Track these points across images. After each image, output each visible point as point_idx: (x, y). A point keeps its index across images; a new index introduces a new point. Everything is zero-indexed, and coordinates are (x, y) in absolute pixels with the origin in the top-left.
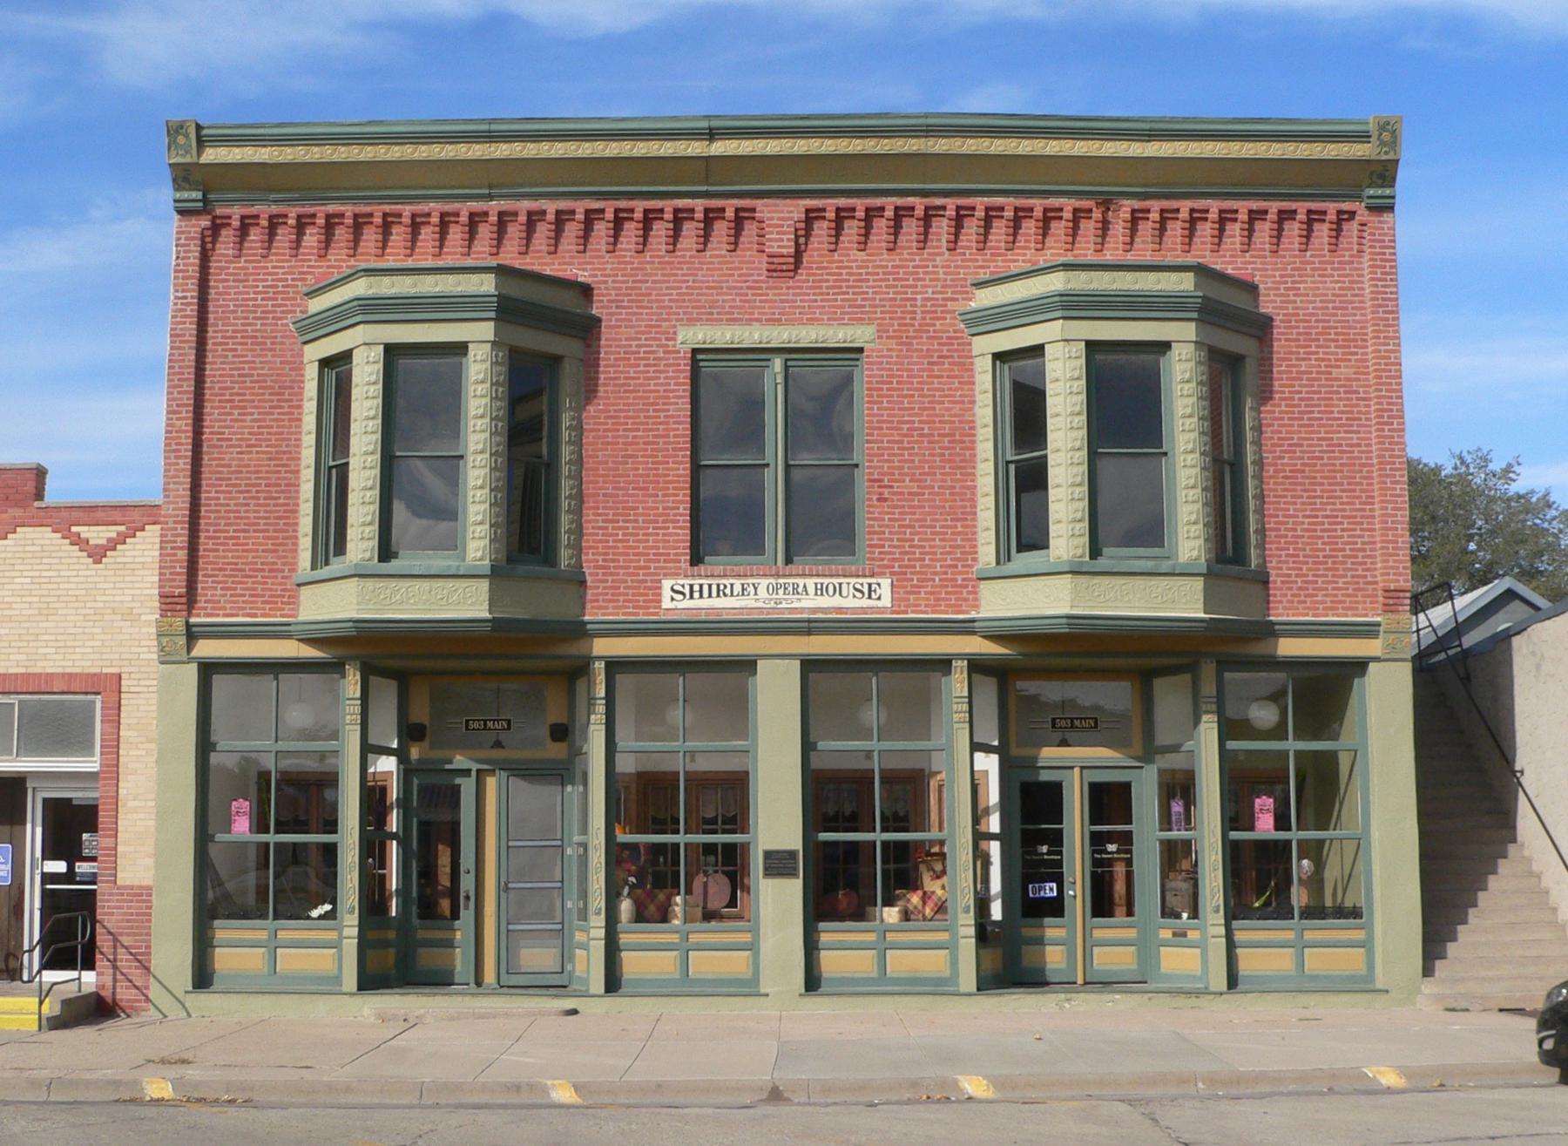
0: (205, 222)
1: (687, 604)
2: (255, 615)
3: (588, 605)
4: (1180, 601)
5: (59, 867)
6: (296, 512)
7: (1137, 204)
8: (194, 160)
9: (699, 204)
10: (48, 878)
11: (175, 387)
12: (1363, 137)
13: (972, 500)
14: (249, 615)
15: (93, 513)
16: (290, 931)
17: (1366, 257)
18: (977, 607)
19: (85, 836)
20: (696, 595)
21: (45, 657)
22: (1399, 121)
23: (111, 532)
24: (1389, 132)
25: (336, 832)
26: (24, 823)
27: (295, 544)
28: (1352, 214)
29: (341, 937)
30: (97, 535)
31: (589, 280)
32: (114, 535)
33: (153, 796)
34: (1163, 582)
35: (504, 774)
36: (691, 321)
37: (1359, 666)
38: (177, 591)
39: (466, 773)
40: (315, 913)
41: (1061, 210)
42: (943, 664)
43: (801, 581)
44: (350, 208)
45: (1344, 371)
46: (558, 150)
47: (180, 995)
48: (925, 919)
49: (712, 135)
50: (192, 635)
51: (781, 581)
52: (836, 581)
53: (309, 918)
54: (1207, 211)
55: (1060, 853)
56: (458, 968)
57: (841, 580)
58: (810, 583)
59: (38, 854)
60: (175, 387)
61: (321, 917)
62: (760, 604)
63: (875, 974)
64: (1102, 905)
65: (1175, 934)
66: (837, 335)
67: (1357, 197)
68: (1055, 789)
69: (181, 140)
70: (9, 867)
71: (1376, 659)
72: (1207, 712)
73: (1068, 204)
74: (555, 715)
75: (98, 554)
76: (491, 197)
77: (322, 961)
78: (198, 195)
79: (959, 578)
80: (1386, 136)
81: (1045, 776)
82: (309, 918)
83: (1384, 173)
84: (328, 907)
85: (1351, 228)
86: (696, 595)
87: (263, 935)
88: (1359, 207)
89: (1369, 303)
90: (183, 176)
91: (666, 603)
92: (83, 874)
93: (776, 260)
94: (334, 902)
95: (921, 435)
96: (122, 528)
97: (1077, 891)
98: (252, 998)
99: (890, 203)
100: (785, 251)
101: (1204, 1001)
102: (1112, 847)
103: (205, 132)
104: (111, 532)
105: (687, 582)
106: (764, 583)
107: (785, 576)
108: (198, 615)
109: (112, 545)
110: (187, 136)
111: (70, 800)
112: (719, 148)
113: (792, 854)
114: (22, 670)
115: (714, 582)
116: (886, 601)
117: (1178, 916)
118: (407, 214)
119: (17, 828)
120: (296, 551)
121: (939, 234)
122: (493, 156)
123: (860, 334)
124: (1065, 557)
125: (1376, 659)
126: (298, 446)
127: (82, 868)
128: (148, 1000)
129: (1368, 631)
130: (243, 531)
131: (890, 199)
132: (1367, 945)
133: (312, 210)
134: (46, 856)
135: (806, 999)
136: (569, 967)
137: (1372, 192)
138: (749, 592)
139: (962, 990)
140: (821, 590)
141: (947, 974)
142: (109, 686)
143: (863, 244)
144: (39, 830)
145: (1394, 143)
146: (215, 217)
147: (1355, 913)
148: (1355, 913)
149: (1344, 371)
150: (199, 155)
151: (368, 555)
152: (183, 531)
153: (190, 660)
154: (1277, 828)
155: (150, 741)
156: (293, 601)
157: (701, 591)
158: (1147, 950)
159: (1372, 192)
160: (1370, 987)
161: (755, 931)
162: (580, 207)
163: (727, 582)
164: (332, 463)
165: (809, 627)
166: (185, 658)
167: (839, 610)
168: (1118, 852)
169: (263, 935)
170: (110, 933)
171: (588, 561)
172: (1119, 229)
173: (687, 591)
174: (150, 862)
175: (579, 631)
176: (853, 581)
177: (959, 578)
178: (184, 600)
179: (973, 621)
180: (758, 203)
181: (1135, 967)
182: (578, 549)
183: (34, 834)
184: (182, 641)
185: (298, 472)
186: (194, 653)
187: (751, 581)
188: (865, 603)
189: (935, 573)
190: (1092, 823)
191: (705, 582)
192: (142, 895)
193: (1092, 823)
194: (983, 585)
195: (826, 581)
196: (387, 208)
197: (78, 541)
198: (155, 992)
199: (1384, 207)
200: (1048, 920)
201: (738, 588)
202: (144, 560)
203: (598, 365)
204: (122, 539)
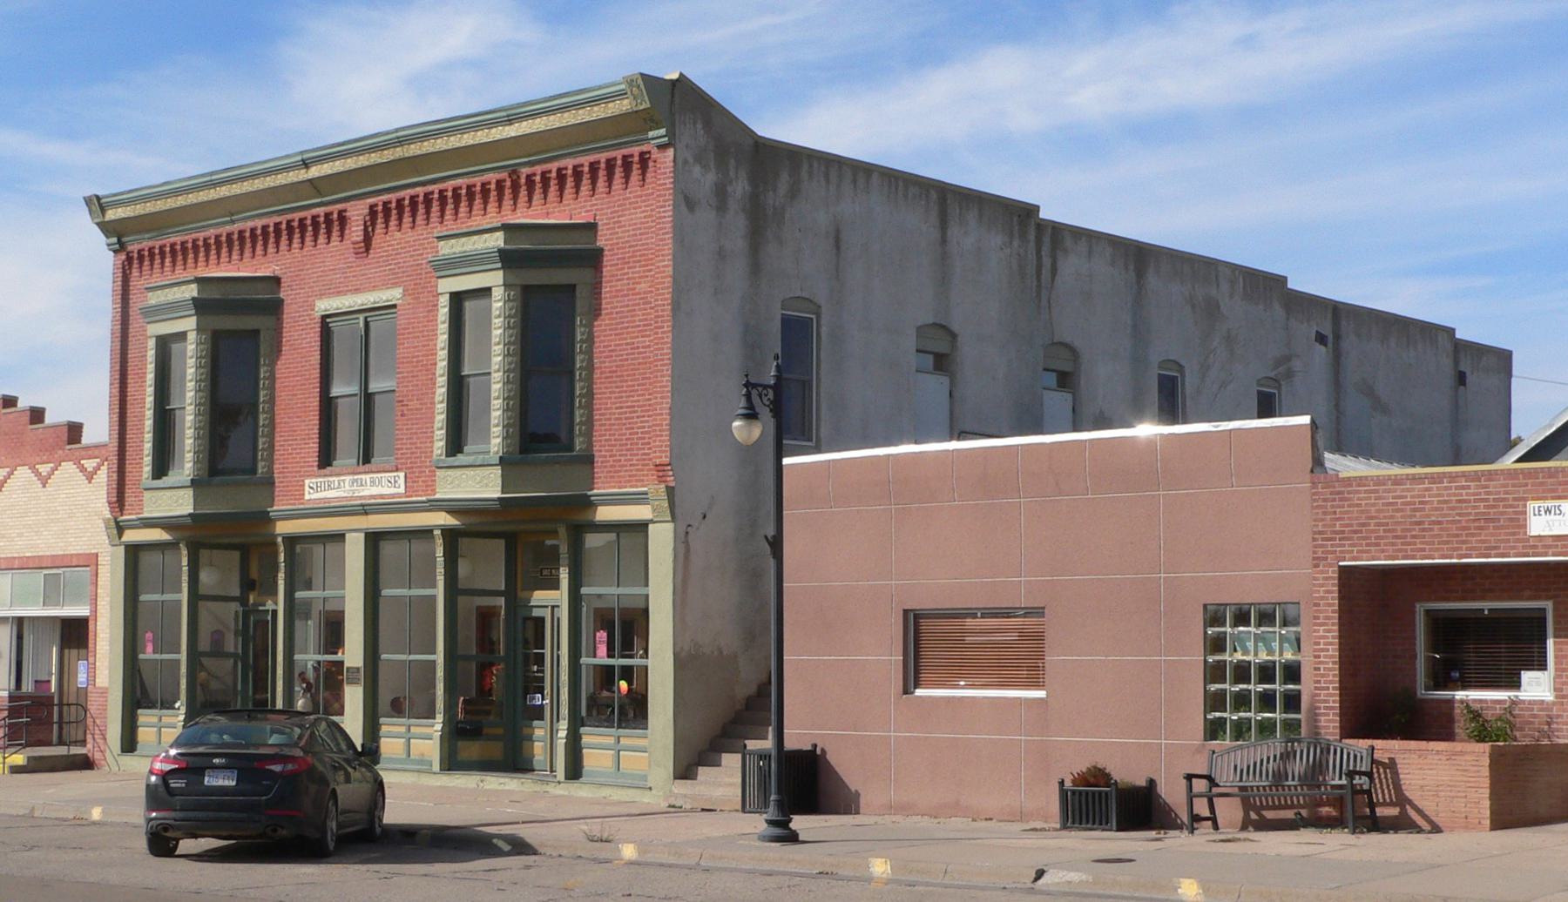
12: (620, 95)
36: (321, 296)
42: (425, 533)
45: (643, 286)
49: (306, 164)
50: (120, 529)
76: (233, 222)
81: (536, 613)
90: (107, 228)
91: (307, 497)
106: (348, 478)
112: (315, 172)
113: (358, 669)
116: (402, 490)
123: (393, 295)
125: (652, 521)
129: (640, 499)
149: (643, 286)
165: (365, 510)
175: (265, 519)
192: (104, 692)
198: (108, 754)
200: (536, 723)
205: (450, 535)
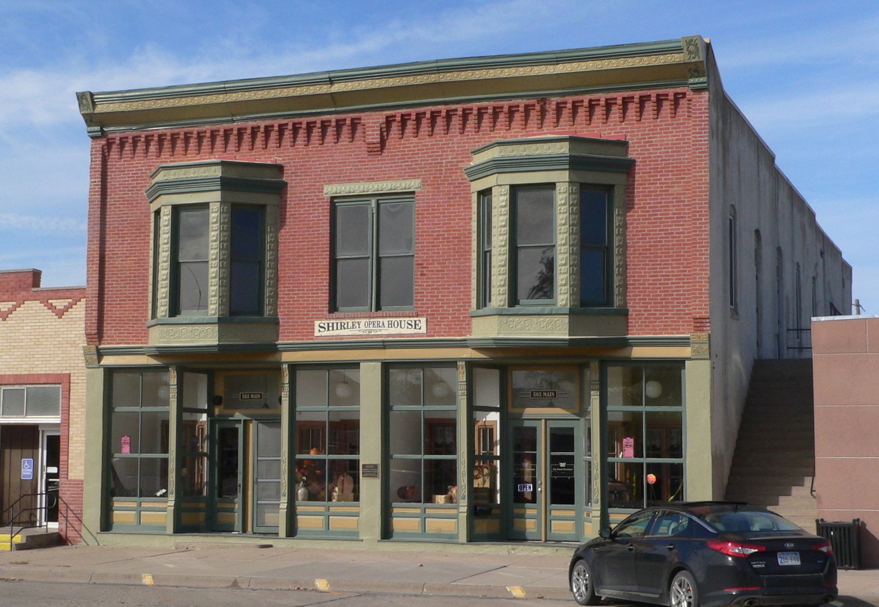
0: (104, 142)
1: (326, 333)
2: (129, 343)
3: (280, 335)
4: (553, 328)
8: (92, 111)
12: (678, 50)
15: (58, 293)
18: (470, 332)
23: (65, 303)
26: (38, 448)
28: (684, 94)
30: (60, 304)
34: (548, 319)
36: (331, 182)
38: (93, 332)
40: (158, 494)
41: (518, 106)
42: (451, 364)
43: (381, 320)
45: (676, 189)
47: (95, 535)
49: (331, 81)
50: (100, 355)
51: (372, 320)
52: (398, 319)
55: (572, 467)
58: (386, 321)
59: (45, 464)
61: (161, 496)
62: (361, 333)
63: (420, 531)
66: (400, 185)
67: (685, 84)
68: (534, 430)
71: (690, 359)
75: (60, 314)
76: (233, 121)
78: (97, 128)
80: (692, 48)
81: (527, 424)
84: (164, 491)
90: (90, 119)
91: (317, 334)
94: (167, 489)
95: (444, 238)
96: (70, 300)
97: (543, 489)
99: (428, 110)
100: (375, 141)
102: (563, 465)
104: (65, 303)
105: (326, 322)
106: (363, 321)
107: (373, 317)
110: (87, 99)
112: (337, 88)
113: (376, 466)
114: (27, 373)
115: (339, 321)
116: (424, 330)
118: (195, 132)
123: (413, 184)
125: (690, 359)
128: (81, 537)
129: (684, 342)
140: (391, 325)
143: (417, 132)
146: (108, 139)
149: (676, 189)
152: (95, 301)
153: (100, 367)
154: (635, 456)
156: (146, 335)
165: (384, 345)
167: (400, 335)
168: (566, 467)
169: (134, 505)
173: (326, 326)
174: (83, 467)
175: (274, 349)
180: (362, 115)
181: (574, 532)
182: (275, 305)
183: (42, 453)
184: (96, 357)
187: (357, 320)
188: (413, 331)
189: (449, 314)
192: (79, 484)
194: (474, 320)
195: (394, 320)
196: (186, 130)
197: (51, 307)
198: (84, 533)
201: (350, 325)
205: (471, 365)
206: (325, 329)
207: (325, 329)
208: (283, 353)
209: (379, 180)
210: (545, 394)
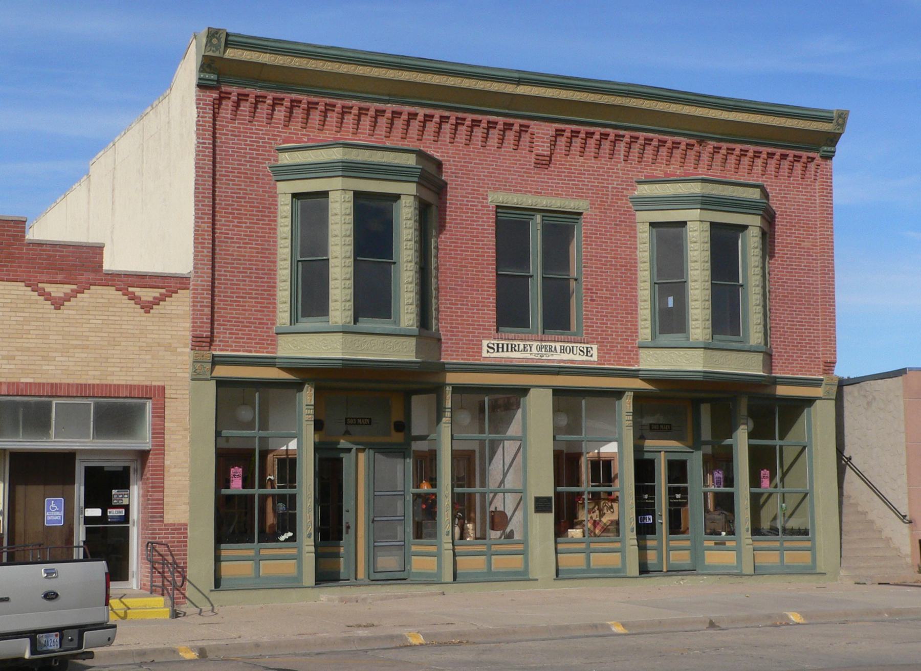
0: (215, 95)
1: (496, 355)
2: (251, 351)
3: (443, 353)
5: (96, 512)
6: (275, 287)
7: (716, 144)
8: (221, 55)
9: (501, 120)
10: (88, 520)
11: (199, 201)
12: (829, 120)
13: (635, 303)
14: (247, 351)
15: (143, 280)
16: (268, 549)
17: (817, 183)
18: (637, 363)
19: (114, 492)
20: (500, 350)
21: (113, 374)
22: (847, 112)
23: (156, 293)
24: (843, 117)
25: (295, 487)
26: (74, 484)
27: (275, 308)
28: (813, 159)
29: (439, 549)
30: (147, 294)
31: (441, 159)
32: (157, 295)
33: (187, 465)
34: (745, 355)
35: (372, 452)
36: (496, 189)
37: (809, 402)
38: (205, 334)
39: (349, 450)
40: (282, 538)
42: (618, 394)
43: (553, 344)
44: (339, 102)
45: (806, 244)
46: (466, 83)
47: (206, 592)
48: (595, 535)
49: (519, 82)
51: (544, 344)
52: (571, 345)
53: (278, 541)
54: (747, 151)
56: (342, 570)
57: (575, 345)
58: (558, 345)
59: (82, 504)
60: (199, 201)
61: (286, 540)
62: (533, 357)
63: (585, 568)
64: (676, 527)
65: (716, 544)
66: (571, 204)
67: (817, 151)
68: (652, 462)
69: (215, 41)
70: (62, 513)
71: (820, 398)
72: (743, 424)
73: (684, 141)
74: (397, 415)
75: (147, 307)
76: (388, 102)
77: (288, 568)
78: (213, 77)
79: (630, 346)
80: (840, 121)
81: (647, 456)
82: (278, 541)
83: (833, 139)
84: (290, 534)
85: (812, 166)
86: (500, 350)
87: (251, 553)
88: (817, 155)
89: (818, 209)
91: (485, 354)
92: (112, 517)
93: (540, 158)
94: (294, 530)
95: (611, 265)
96: (163, 291)
97: (663, 520)
98: (270, 591)
99: (598, 130)
100: (546, 153)
101: (744, 579)
102: (678, 496)
103: (230, 38)
104: (156, 293)
105: (496, 342)
107: (545, 341)
108: (215, 350)
109: (157, 301)
110: (219, 39)
111: (103, 467)
113: (549, 499)
114: (97, 382)
115: (510, 342)
116: (595, 358)
117: (720, 534)
118: (339, 105)
119: (67, 487)
120: (275, 312)
121: (619, 151)
122: (400, 78)
124: (701, 339)
125: (820, 398)
126: (275, 246)
127: (113, 513)
128: (185, 597)
129: (816, 383)
130: (242, 297)
131: (597, 129)
132: (812, 549)
133: (282, 96)
134: (89, 504)
135: (317, 591)
136: (408, 568)
137: (825, 148)
138: (528, 349)
139: (446, 581)
140: (563, 350)
141: (620, 566)
142: (157, 394)
144: (82, 488)
145: (842, 125)
146: (221, 92)
147: (805, 532)
148: (805, 532)
149: (806, 244)
150: (224, 52)
151: (411, 322)
152: (207, 295)
153: (212, 378)
155: (185, 430)
156: (274, 343)
157: (503, 348)
158: (697, 553)
159: (825, 148)
160: (813, 571)
161: (812, 540)
162: (438, 113)
163: (516, 343)
164: (299, 259)
166: (209, 377)
167: (572, 361)
168: (681, 498)
169: (251, 553)
170: (161, 555)
171: (443, 327)
172: (705, 157)
173: (495, 348)
174: (186, 508)
176: (579, 345)
177: (630, 346)
178: (208, 340)
179: (639, 370)
180: (532, 123)
181: (689, 562)
183: (79, 490)
184: (209, 366)
185: (275, 262)
186: (213, 375)
187: (528, 343)
188: (585, 358)
189: (618, 343)
190: (669, 482)
191: (505, 342)
193: (669, 482)
194: (641, 351)
195: (566, 345)
196: (328, 101)
197: (133, 297)
199: (828, 157)
200: (648, 536)
201: (522, 347)
202: (180, 314)
203: (446, 211)
204: (162, 298)
205: (639, 397)
206: (493, 349)
207: (493, 349)
208: (448, 374)
209: (547, 194)
210: (359, 421)
